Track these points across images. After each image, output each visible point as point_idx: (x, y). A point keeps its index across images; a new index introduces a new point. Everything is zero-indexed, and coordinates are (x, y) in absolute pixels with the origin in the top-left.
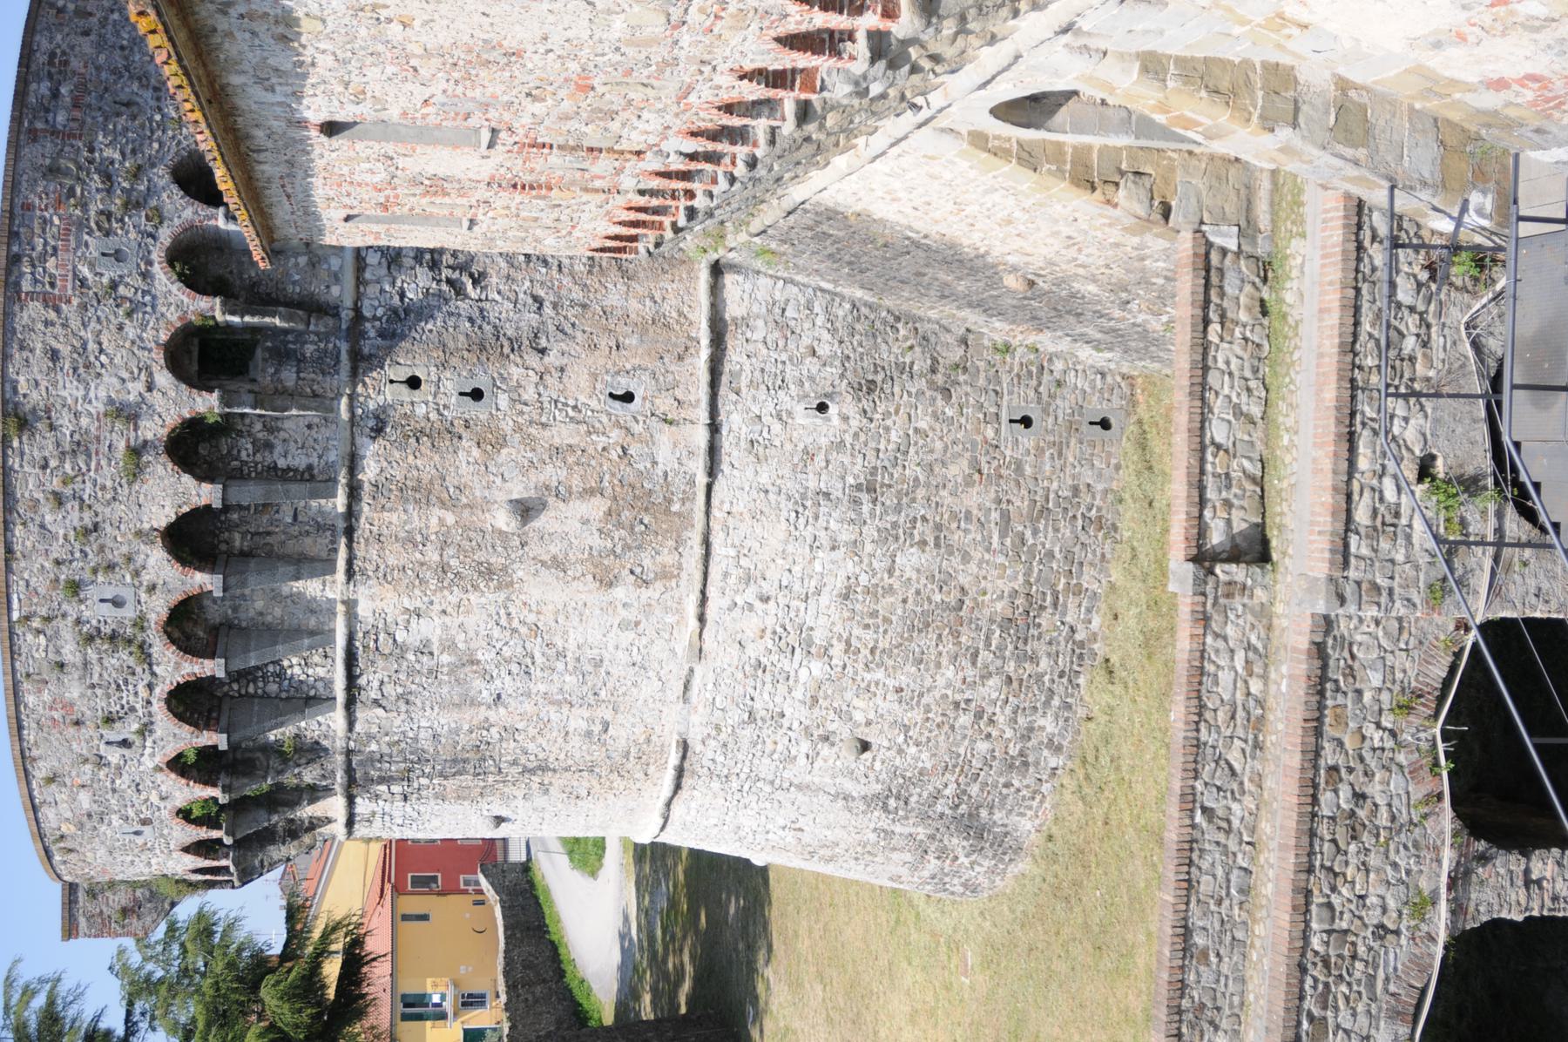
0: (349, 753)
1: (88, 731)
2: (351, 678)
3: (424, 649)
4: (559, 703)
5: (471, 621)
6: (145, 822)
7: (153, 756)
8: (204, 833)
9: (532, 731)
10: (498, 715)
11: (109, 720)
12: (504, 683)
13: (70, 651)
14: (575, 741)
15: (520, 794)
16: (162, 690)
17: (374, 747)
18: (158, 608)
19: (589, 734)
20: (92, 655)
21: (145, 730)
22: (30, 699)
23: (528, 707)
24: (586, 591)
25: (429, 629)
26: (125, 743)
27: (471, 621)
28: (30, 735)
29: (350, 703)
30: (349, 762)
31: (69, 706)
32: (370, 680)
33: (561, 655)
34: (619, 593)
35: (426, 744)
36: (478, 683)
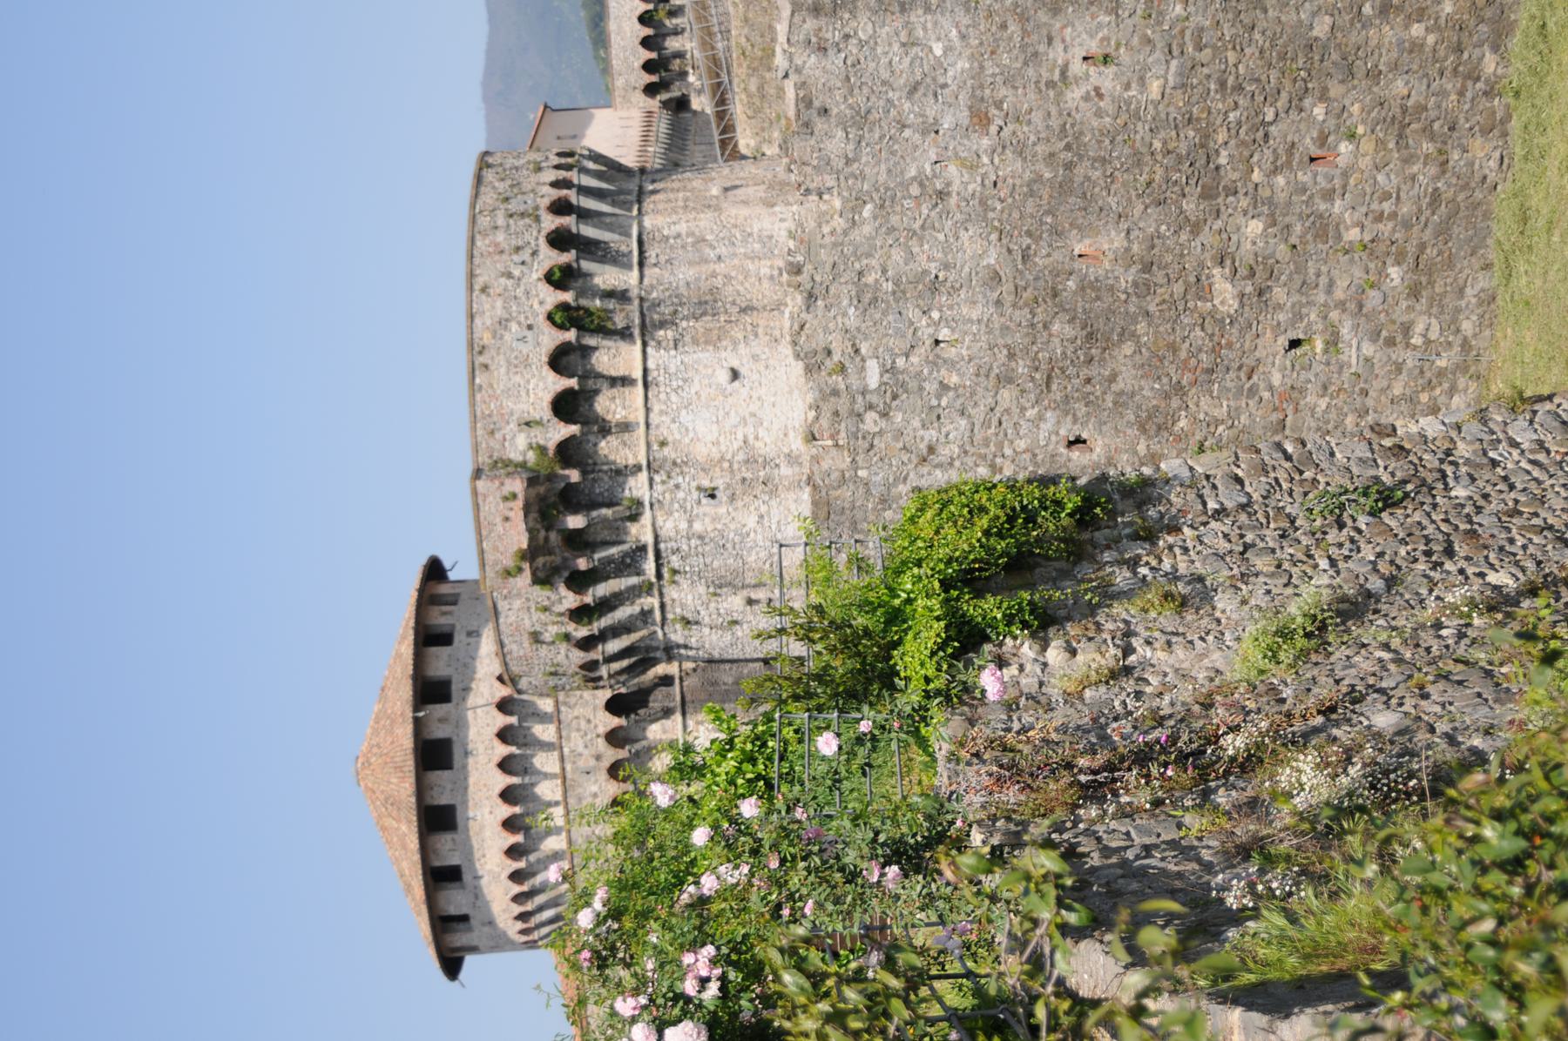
0: (642, 299)
1: (505, 257)
2: (641, 252)
3: (678, 236)
4: (752, 258)
5: (702, 224)
6: (530, 327)
7: (537, 273)
8: (562, 174)
9: (741, 278)
10: (720, 268)
11: (518, 249)
12: (722, 250)
13: (501, 221)
14: (766, 284)
15: (740, 336)
16: (544, 233)
17: (654, 295)
18: (546, 202)
19: (772, 278)
20: (511, 221)
21: (534, 253)
22: (479, 243)
23: (736, 261)
24: (761, 210)
25: (682, 228)
26: (523, 263)
27: (702, 224)
28: (477, 261)
29: (641, 264)
30: (641, 307)
31: (497, 245)
32: (651, 254)
33: (750, 235)
34: (777, 209)
35: (683, 290)
36: (708, 250)
